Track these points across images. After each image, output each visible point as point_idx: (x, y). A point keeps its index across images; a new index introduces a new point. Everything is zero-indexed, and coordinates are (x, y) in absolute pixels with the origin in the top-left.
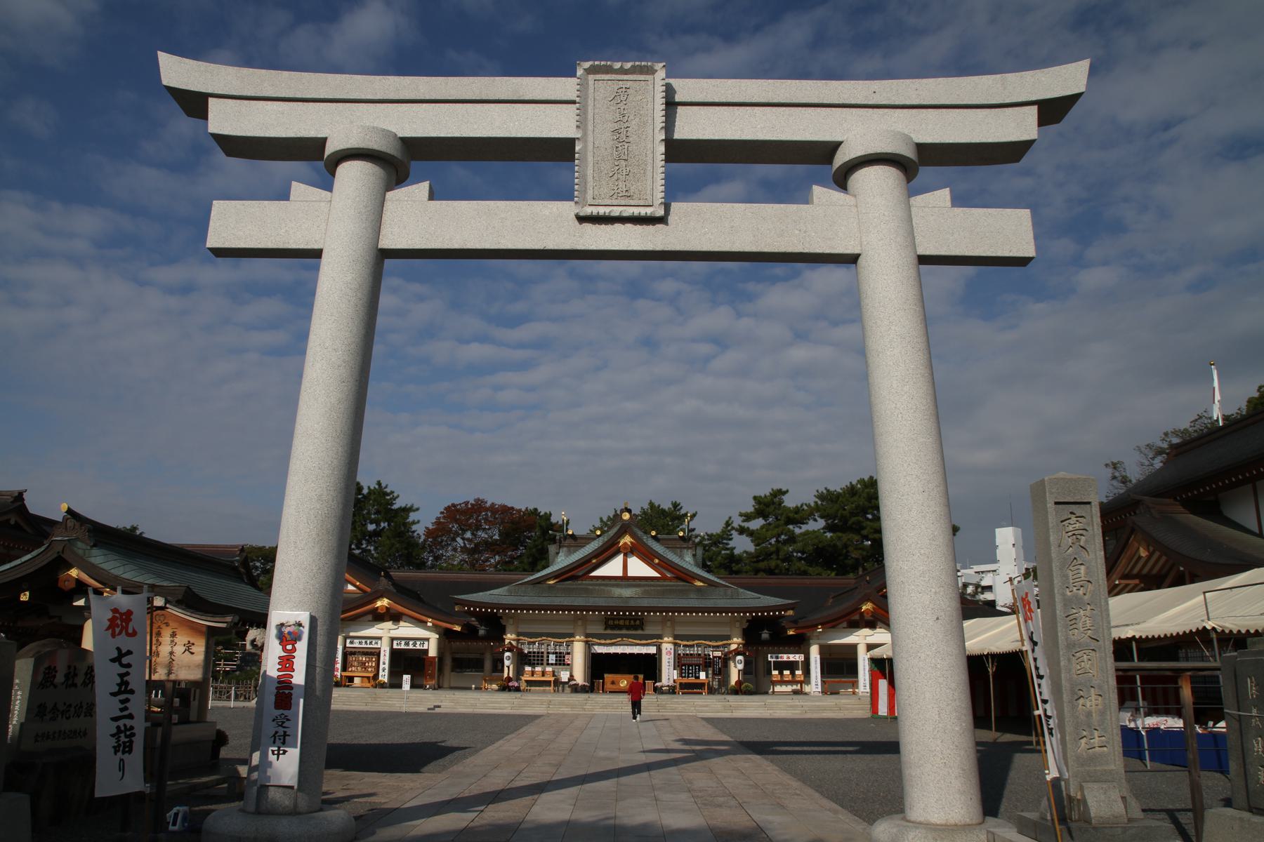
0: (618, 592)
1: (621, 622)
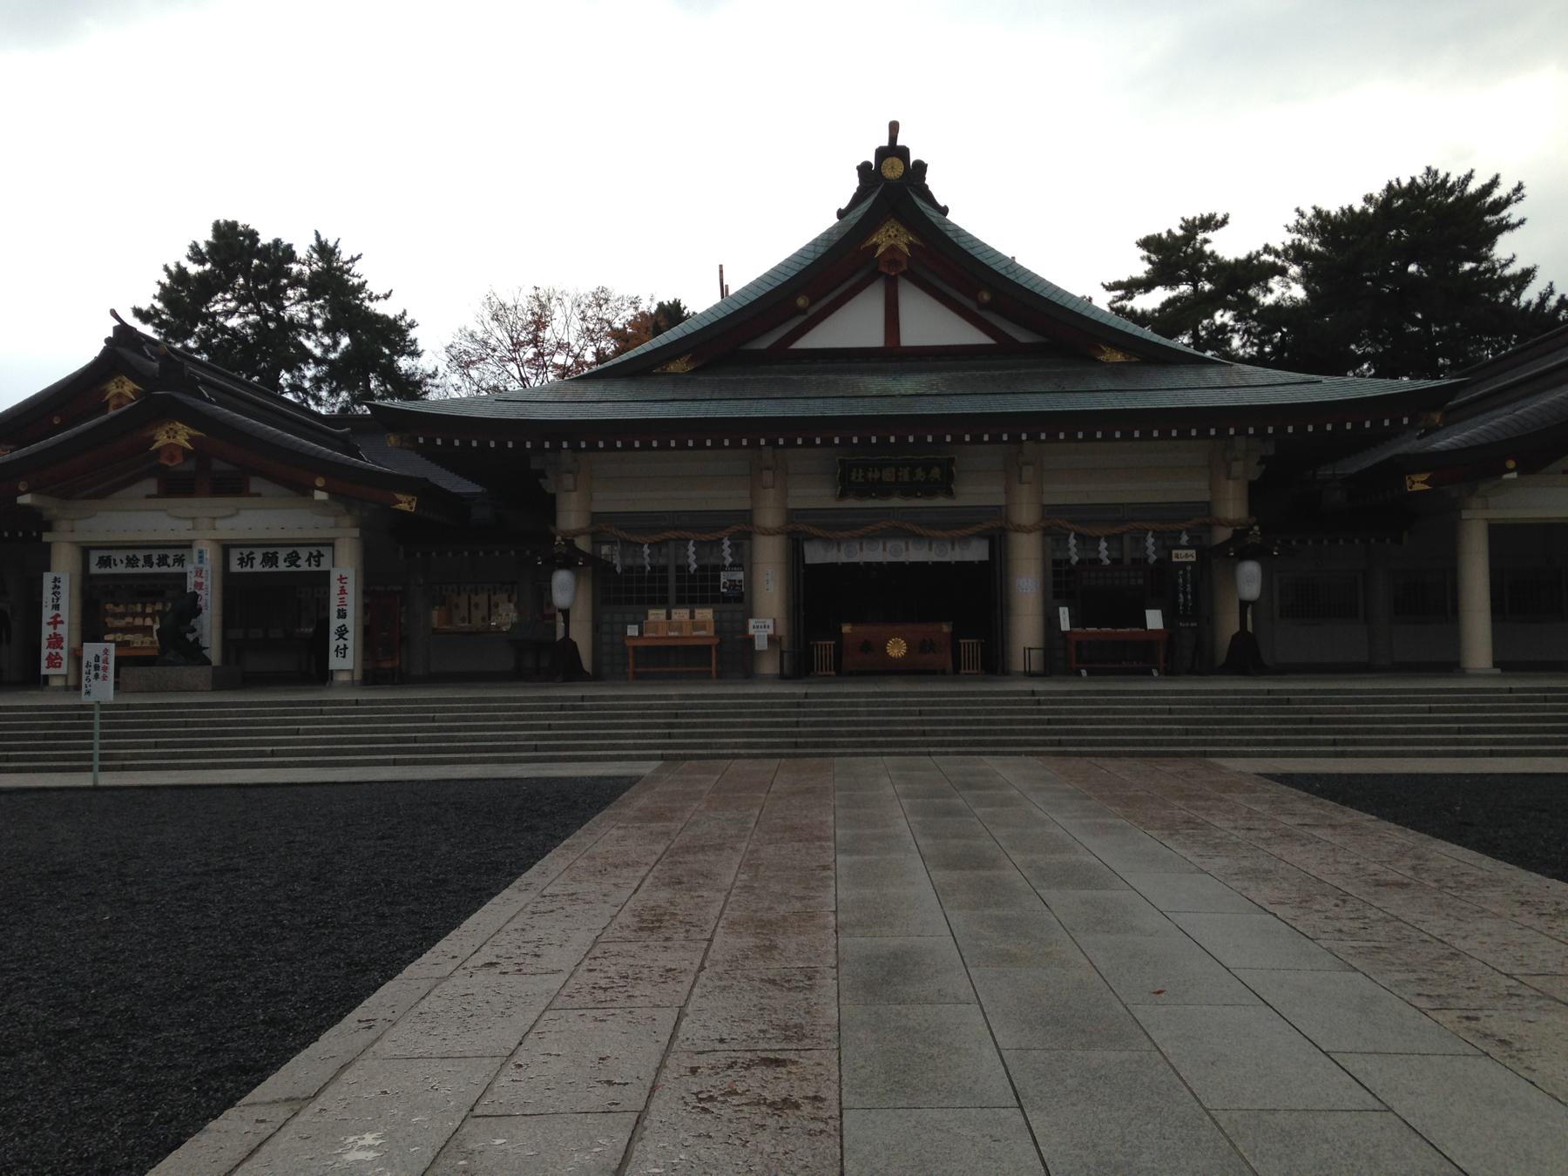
0: (875, 384)
1: (888, 475)
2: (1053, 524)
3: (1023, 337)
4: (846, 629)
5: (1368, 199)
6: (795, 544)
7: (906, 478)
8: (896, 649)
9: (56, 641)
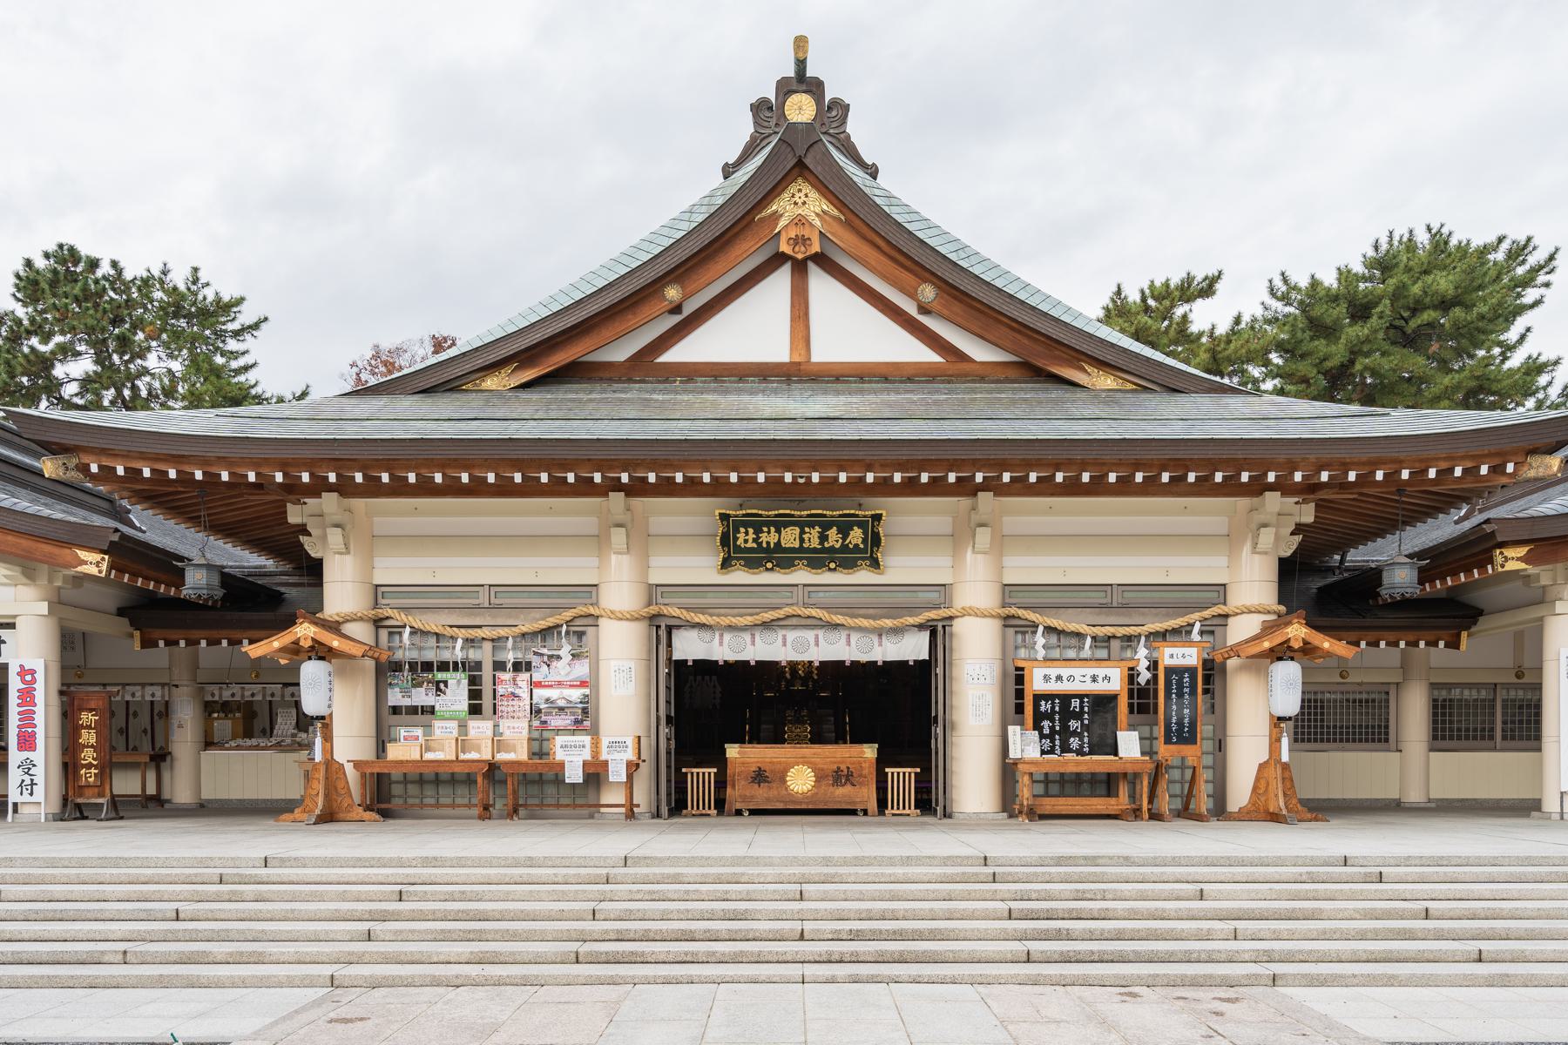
1: (790, 537)
2: (1018, 614)
3: (980, 352)
4: (732, 751)
6: (661, 629)
7: (815, 543)
8: (801, 781)
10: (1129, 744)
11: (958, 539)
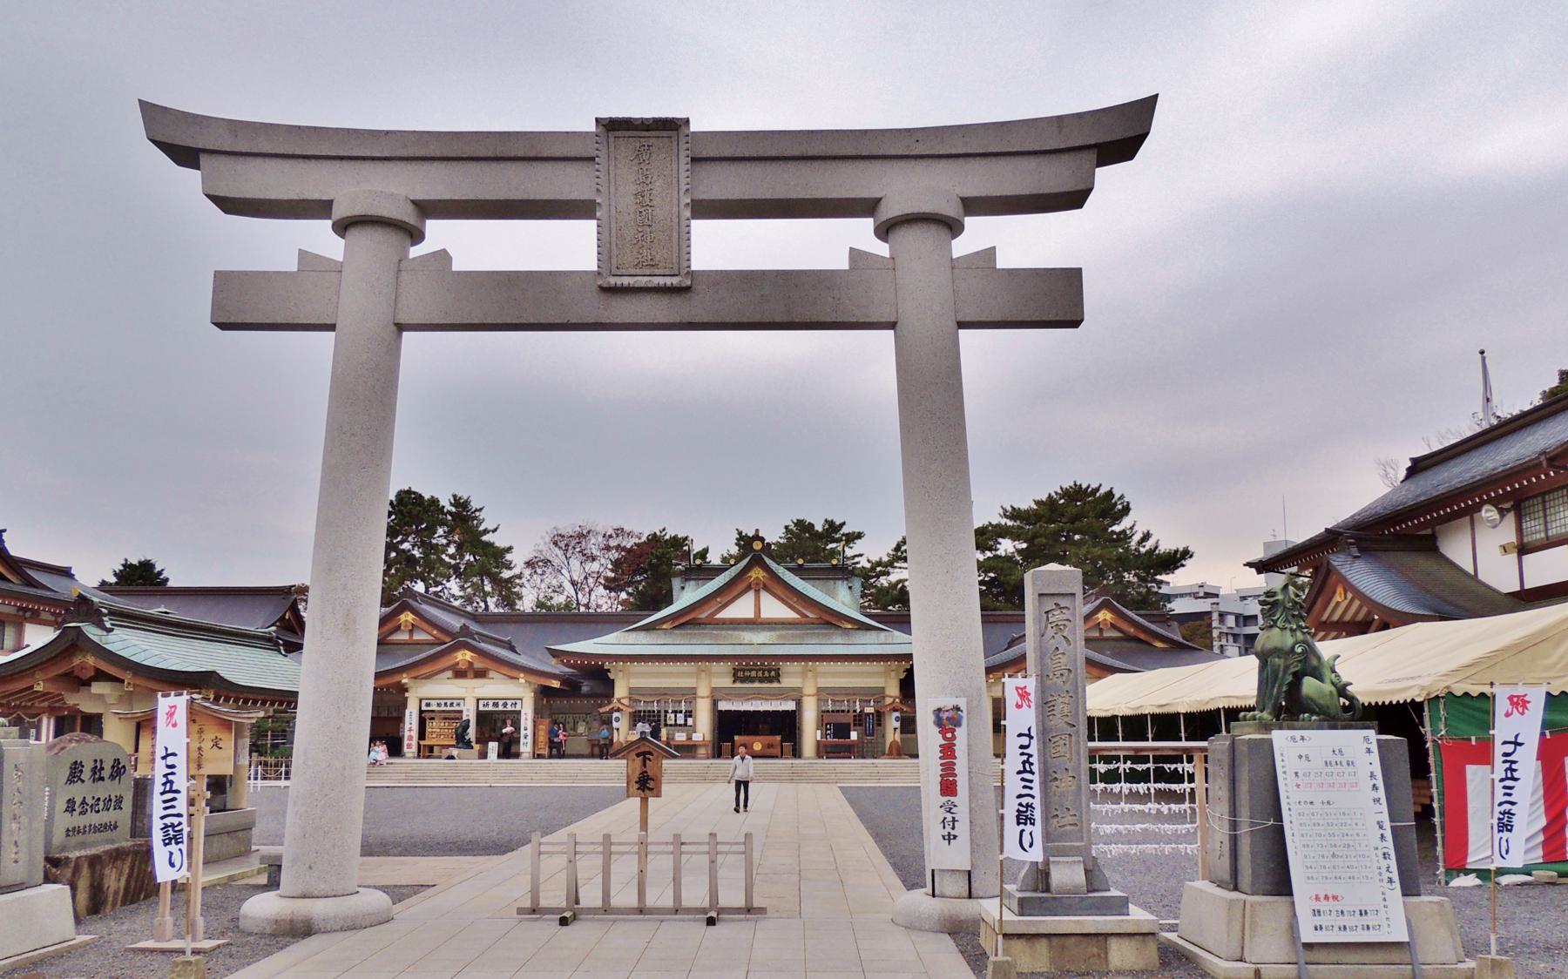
1: (753, 674)
2: (822, 693)
5: (1037, 503)
6: (715, 703)
9: (410, 738)
10: (854, 735)
11: (804, 674)
